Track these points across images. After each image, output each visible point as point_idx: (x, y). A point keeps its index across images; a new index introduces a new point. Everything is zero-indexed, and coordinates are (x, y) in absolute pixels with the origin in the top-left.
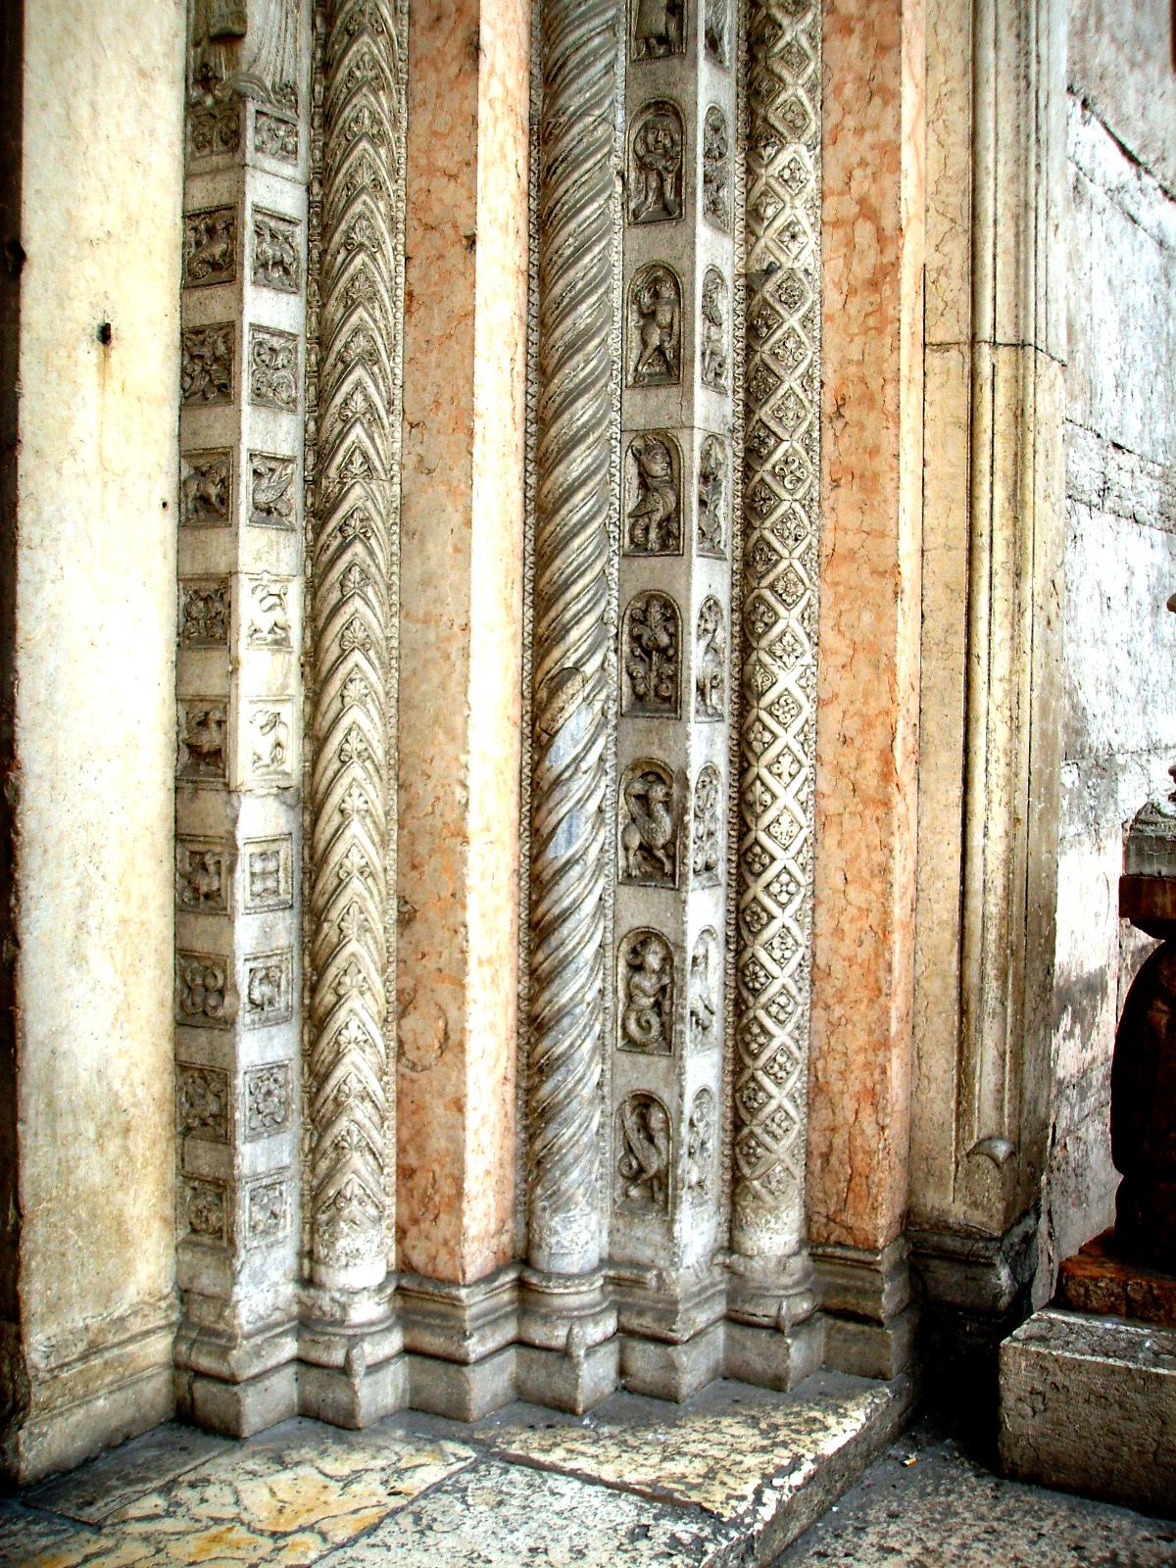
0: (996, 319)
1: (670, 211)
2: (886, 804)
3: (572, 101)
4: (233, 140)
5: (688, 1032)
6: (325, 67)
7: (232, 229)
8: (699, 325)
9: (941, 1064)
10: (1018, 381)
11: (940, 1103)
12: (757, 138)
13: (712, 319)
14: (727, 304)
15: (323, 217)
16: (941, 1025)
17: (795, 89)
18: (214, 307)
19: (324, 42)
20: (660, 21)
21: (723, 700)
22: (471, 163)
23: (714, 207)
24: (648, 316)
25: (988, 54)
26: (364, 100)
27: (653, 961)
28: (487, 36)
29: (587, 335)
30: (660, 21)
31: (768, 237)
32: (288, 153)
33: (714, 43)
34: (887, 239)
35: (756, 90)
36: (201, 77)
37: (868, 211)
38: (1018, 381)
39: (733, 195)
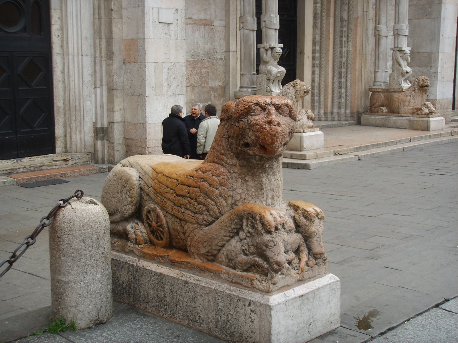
0: (364, 52)
1: (341, 47)
2: (355, 84)
3: (336, 41)
4: (315, 45)
5: (342, 98)
6: (321, 40)
7: (315, 50)
8: (343, 54)
9: (360, 101)
10: (365, 56)
11: (360, 104)
12: (348, 42)
13: (344, 54)
14: (346, 53)
15: (320, 49)
16: (360, 99)
17: (350, 39)
18: (314, 55)
19: (321, 38)
20: (341, 35)
21: (345, 77)
22: (329, 46)
23: (345, 47)
24: (340, 54)
25: (364, 35)
26: (323, 42)
27: (340, 93)
28: (330, 38)
29: (336, 55)
30: (341, 35)
31: (348, 48)
32: (318, 45)
33: (345, 36)
34: (356, 48)
35: (348, 39)
36: (313, 41)
37: (355, 46)
38: (365, 56)
39: (346, 45)
